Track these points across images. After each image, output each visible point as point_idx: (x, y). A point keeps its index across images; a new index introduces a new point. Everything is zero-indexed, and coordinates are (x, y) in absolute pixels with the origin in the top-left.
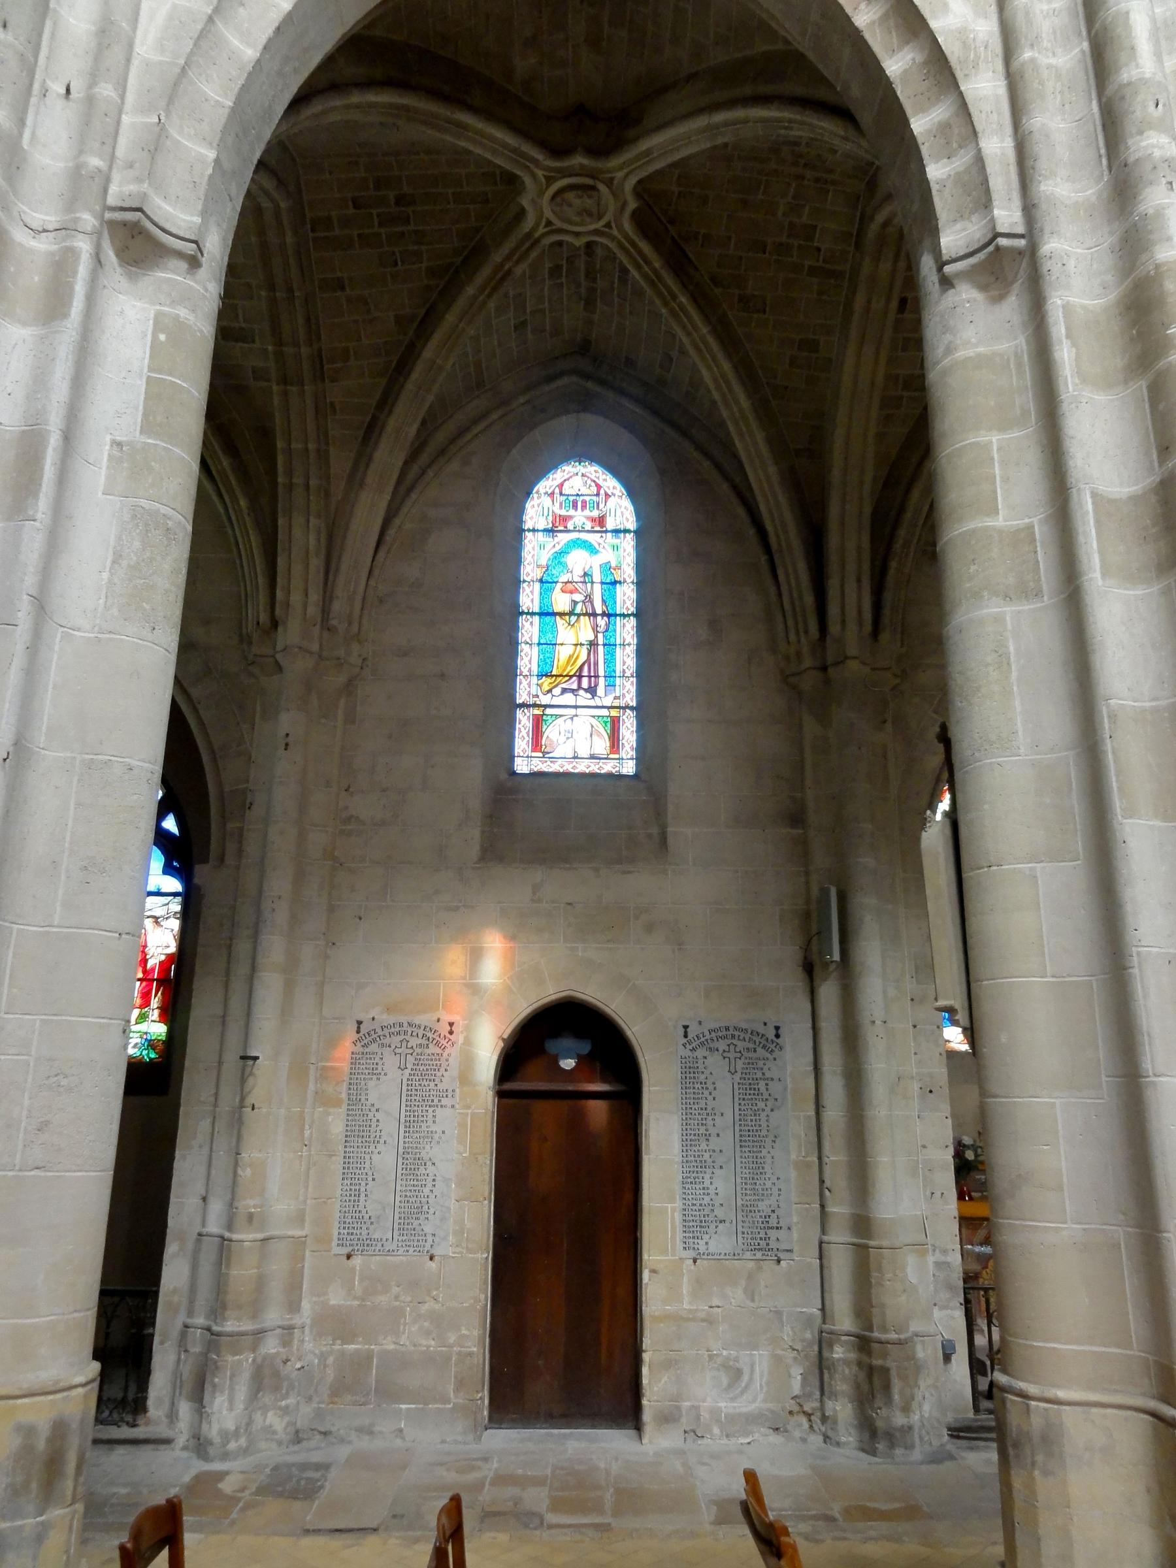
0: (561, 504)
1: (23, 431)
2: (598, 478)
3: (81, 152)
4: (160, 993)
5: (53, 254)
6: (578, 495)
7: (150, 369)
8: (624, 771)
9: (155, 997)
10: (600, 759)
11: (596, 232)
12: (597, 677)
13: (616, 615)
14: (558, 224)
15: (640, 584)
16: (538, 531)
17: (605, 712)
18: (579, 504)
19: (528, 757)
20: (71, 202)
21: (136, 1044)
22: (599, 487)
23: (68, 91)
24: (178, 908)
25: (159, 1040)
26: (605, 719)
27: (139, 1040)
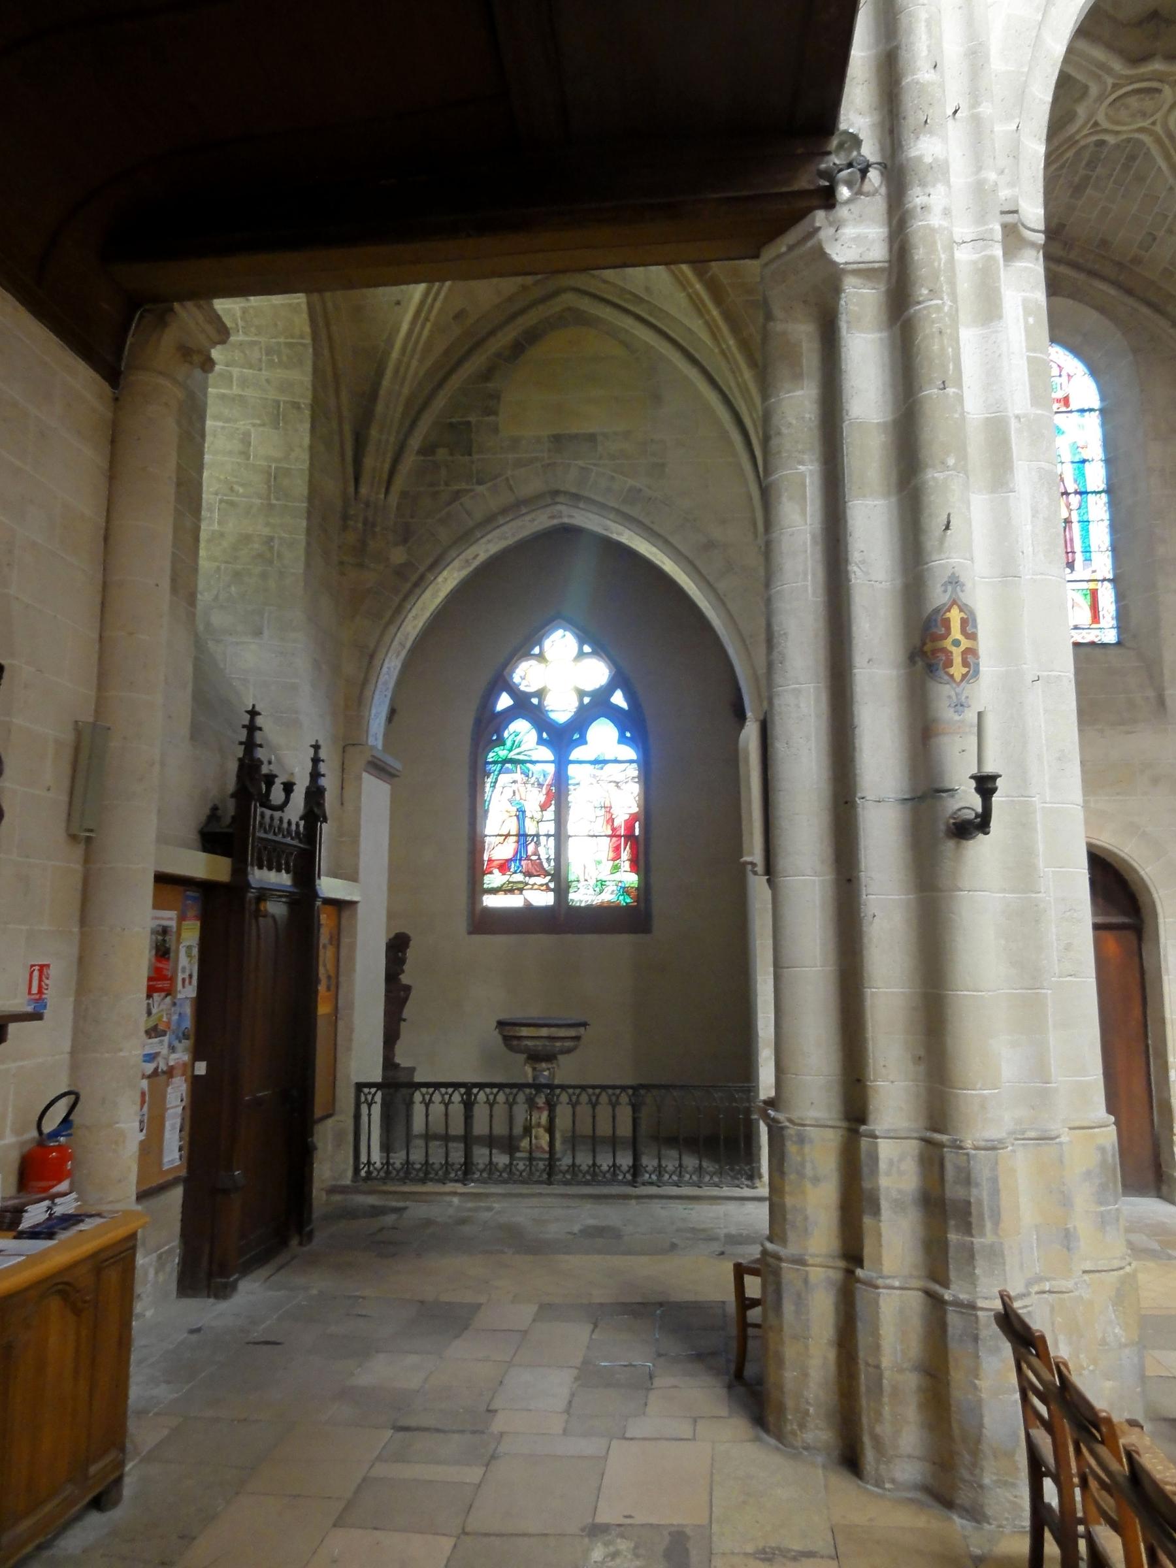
1: (987, 418)
3: (979, 169)
4: (628, 847)
5: (975, 263)
7: (1028, 350)
8: (1106, 640)
9: (625, 849)
10: (1083, 629)
11: (1141, 130)
12: (1073, 552)
13: (1087, 493)
14: (1105, 124)
15: (1109, 461)
17: (1085, 585)
20: (981, 218)
21: (613, 891)
23: (956, 112)
24: (636, 773)
25: (632, 888)
27: (615, 888)
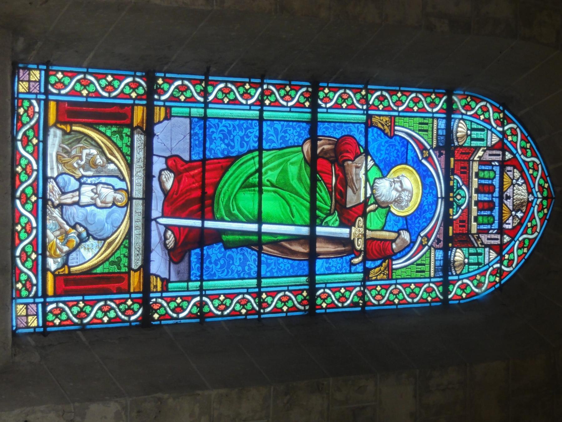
0: (489, 163)
2: (525, 232)
6: (501, 191)
16: (449, 120)
17: (137, 262)
18: (485, 197)
19: (47, 92)
22: (513, 233)
26: (125, 261)
